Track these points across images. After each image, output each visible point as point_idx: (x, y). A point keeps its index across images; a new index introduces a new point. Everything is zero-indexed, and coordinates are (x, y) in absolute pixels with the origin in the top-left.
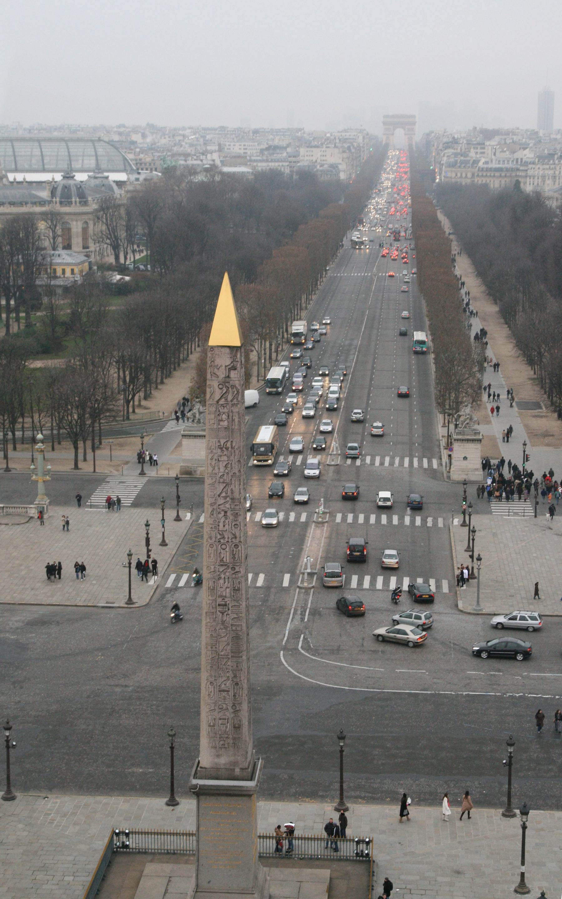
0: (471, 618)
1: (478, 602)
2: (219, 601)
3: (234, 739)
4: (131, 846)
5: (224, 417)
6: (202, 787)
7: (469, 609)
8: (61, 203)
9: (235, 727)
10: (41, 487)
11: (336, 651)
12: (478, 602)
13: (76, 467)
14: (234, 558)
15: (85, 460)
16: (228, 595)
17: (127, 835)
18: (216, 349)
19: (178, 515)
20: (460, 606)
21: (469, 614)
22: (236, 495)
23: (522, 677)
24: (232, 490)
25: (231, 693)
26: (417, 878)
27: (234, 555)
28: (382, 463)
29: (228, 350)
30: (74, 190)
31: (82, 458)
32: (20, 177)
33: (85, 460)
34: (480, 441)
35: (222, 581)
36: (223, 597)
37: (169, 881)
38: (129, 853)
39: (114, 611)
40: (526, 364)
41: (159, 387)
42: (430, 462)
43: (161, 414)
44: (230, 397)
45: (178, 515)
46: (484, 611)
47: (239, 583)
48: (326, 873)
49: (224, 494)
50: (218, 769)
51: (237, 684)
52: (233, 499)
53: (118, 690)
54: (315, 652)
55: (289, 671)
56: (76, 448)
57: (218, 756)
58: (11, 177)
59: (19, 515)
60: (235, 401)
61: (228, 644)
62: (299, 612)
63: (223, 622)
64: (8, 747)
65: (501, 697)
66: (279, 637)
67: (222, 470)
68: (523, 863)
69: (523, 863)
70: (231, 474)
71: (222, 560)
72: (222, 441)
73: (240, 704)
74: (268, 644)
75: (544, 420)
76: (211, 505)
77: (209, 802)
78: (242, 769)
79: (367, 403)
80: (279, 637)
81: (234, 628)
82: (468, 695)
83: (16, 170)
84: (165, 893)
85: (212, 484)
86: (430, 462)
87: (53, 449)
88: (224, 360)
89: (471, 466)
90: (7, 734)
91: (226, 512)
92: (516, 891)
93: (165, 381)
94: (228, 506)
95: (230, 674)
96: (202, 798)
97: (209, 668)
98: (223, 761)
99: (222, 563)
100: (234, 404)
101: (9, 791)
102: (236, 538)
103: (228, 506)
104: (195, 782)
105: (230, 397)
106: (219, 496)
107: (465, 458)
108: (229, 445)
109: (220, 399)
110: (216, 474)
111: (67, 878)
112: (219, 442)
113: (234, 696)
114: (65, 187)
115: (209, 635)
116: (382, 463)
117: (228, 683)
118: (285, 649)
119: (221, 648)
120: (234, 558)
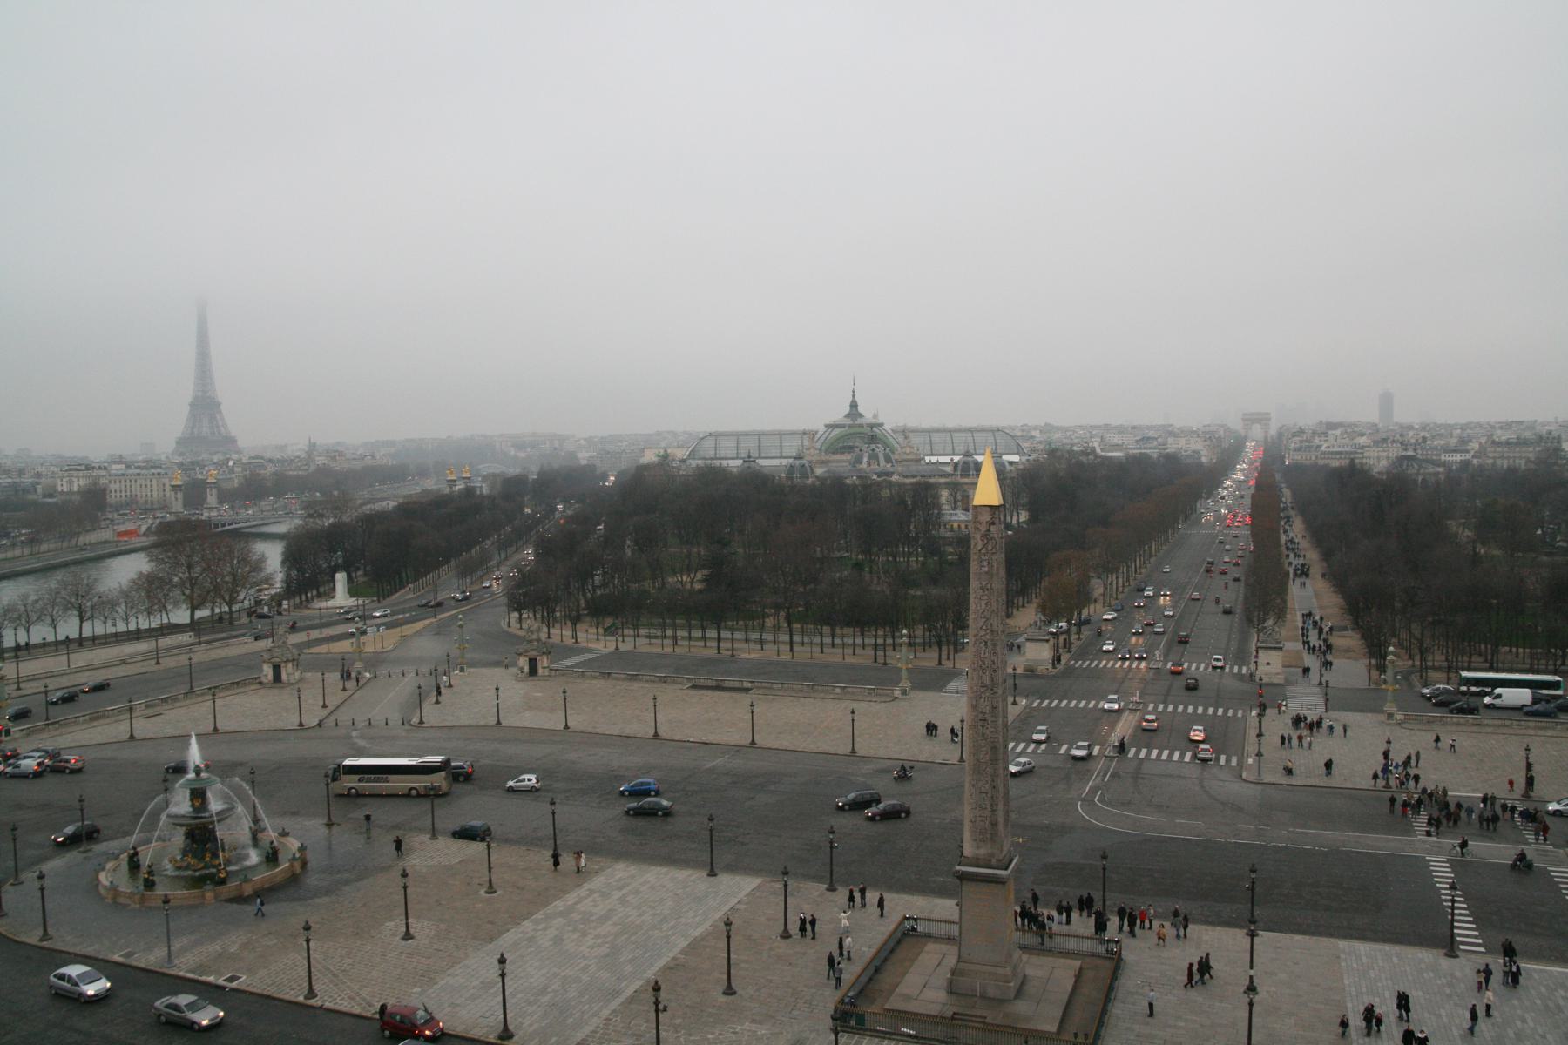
0: (1252, 786)
1: (1259, 773)
2: (980, 717)
4: (919, 930)
5: (985, 563)
7: (1251, 778)
8: (961, 475)
9: (992, 824)
10: (904, 674)
11: (1126, 804)
12: (1259, 773)
13: (940, 663)
14: (993, 681)
15: (948, 659)
17: (915, 920)
18: (979, 510)
19: (1015, 700)
20: (1244, 775)
21: (1251, 782)
22: (995, 628)
23: (1289, 832)
24: (991, 624)
25: (989, 795)
26: (1158, 975)
27: (992, 678)
28: (1197, 668)
29: (988, 509)
30: (972, 465)
31: (946, 657)
32: (934, 459)
33: (948, 659)
34: (1281, 649)
35: (983, 700)
37: (943, 957)
38: (918, 936)
39: (948, 767)
40: (1335, 592)
41: (1021, 609)
42: (1240, 669)
43: (1017, 629)
44: (990, 548)
45: (1015, 700)
46: (1265, 781)
47: (997, 702)
48: (1077, 964)
49: (984, 627)
50: (978, 859)
51: (994, 787)
52: (992, 631)
53: (937, 821)
54: (1109, 804)
55: (1083, 817)
56: (940, 650)
57: (978, 848)
58: (927, 459)
59: (887, 695)
60: (994, 551)
61: (986, 754)
62: (1101, 774)
63: (983, 735)
64: (831, 848)
65: (1266, 846)
66: (1081, 791)
67: (983, 605)
68: (1251, 968)
69: (1251, 968)
70: (990, 611)
71: (982, 683)
72: (984, 583)
73: (997, 805)
74: (1070, 796)
75: (1348, 639)
76: (975, 636)
78: (997, 860)
79: (1194, 624)
80: (1081, 791)
81: (992, 740)
82: (1236, 843)
83: (932, 455)
84: (938, 966)
85: (975, 619)
86: (1240, 669)
87: (924, 651)
88: (986, 517)
89: (1274, 671)
90: (831, 837)
91: (986, 642)
93: (1026, 605)
94: (988, 637)
95: (989, 779)
96: (965, 882)
97: (971, 773)
98: (982, 852)
99: (983, 685)
100: (993, 553)
101: (831, 883)
102: (994, 664)
103: (988, 637)
104: (958, 868)
105: (990, 548)
106: (981, 628)
107: (1268, 664)
108: (989, 586)
109: (982, 549)
110: (978, 610)
111: (863, 949)
112: (981, 584)
113: (992, 797)
114: (965, 463)
115: (971, 745)
116: (1197, 668)
118: (1083, 800)
119: (981, 756)
120: (993, 681)
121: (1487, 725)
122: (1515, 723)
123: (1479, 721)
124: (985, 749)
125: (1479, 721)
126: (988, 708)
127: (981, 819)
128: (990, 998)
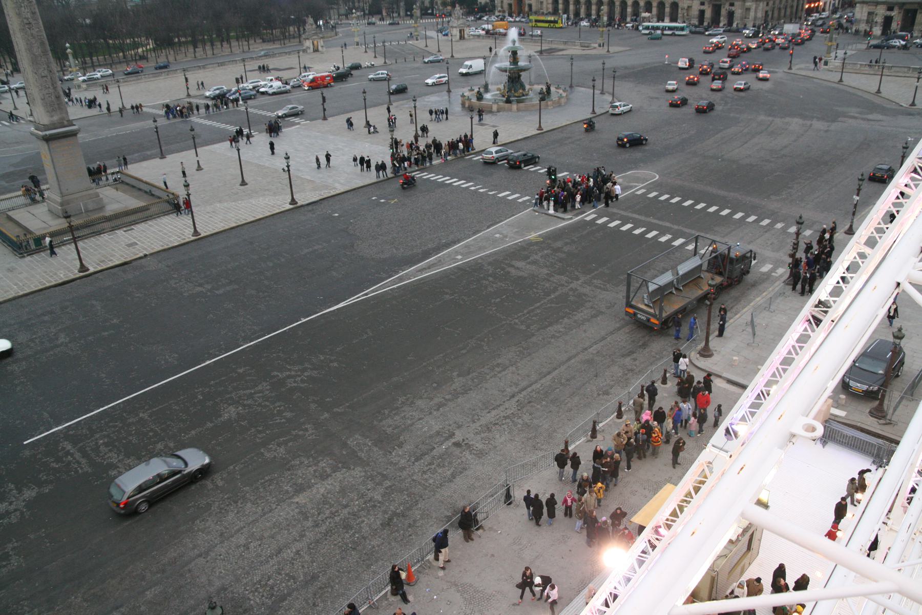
3: (58, 104)
6: (51, 135)
9: (56, 97)
16: (29, 17)
25: (49, 77)
36: (27, 19)
47: (34, 8)
51: (51, 71)
57: (52, 116)
63: (32, 35)
73: (56, 83)
77: (55, 144)
92: (197, 170)
95: (45, 66)
96: (50, 142)
98: (56, 118)
117: (46, 72)
121: (130, 81)
122: (143, 77)
123: (126, 80)
124: (36, 45)
125: (126, 80)
126: (29, 14)
127: (47, 96)
128: (91, 211)
